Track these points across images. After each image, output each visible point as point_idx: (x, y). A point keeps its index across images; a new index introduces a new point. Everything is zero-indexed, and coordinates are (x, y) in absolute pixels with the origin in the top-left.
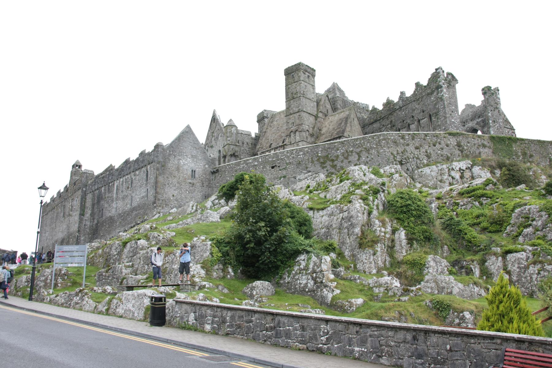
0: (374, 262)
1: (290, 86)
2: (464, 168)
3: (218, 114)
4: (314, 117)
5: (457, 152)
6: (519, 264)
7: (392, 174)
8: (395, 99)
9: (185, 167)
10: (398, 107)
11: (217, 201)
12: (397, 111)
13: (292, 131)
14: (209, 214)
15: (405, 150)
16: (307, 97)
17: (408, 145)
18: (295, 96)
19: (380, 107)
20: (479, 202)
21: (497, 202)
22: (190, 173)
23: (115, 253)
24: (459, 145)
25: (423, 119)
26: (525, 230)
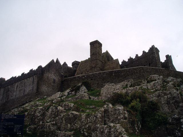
3: (59, 60)
8: (134, 57)
11: (70, 92)
14: (83, 95)
19: (127, 61)
23: (39, 115)
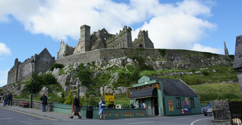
9: (44, 61)
22: (46, 62)
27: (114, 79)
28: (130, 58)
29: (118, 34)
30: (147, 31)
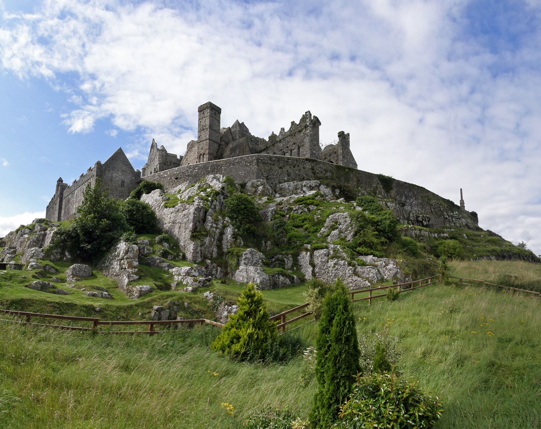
0: (201, 252)
1: (201, 120)
2: (314, 186)
4: (218, 145)
5: (311, 174)
6: (322, 258)
7: (258, 186)
10: (278, 140)
12: (278, 143)
13: (201, 154)
15: (271, 169)
16: (213, 128)
17: (274, 165)
18: (205, 128)
20: (307, 209)
21: (320, 209)
24: (313, 169)
25: (294, 149)
26: (333, 232)
27: (341, 232)
28: (327, 185)
29: (286, 131)
30: (348, 134)
